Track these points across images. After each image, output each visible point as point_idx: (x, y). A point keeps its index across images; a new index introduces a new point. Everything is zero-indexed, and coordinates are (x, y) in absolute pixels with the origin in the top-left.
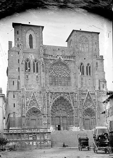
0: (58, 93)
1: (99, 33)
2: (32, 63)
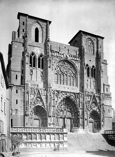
0: (64, 92)
2: (37, 57)
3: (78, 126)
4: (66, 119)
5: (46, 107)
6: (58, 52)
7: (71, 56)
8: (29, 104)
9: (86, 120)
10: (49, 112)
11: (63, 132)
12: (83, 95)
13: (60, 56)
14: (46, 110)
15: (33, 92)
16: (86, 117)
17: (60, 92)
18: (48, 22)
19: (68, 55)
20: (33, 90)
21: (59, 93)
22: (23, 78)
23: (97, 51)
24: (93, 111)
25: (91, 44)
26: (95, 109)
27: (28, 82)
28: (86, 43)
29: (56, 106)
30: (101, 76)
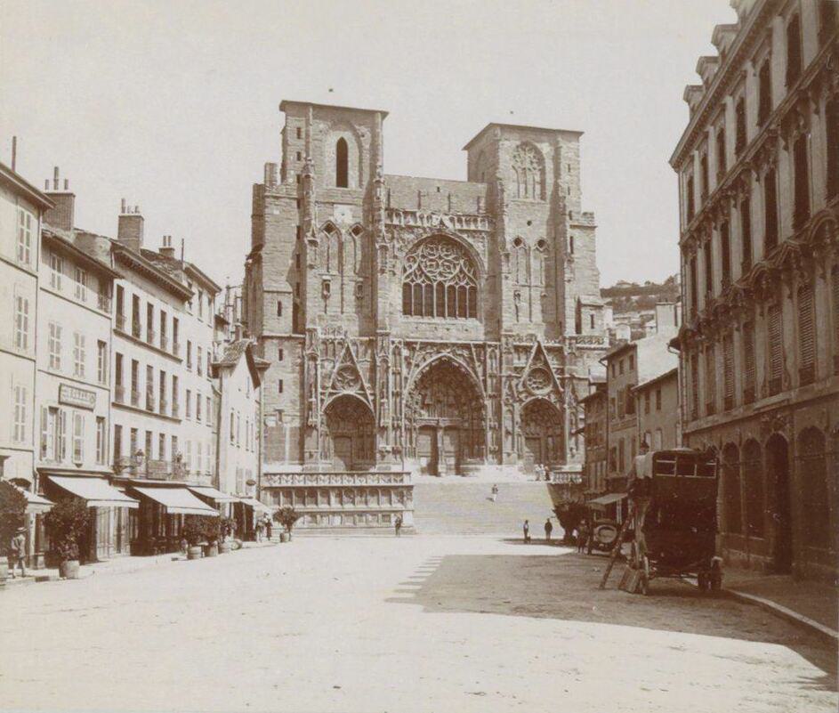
1: (581, 133)
3: (480, 455)
4: (440, 433)
5: (371, 398)
6: (413, 214)
7: (456, 218)
8: (316, 390)
9: (508, 433)
10: (380, 414)
11: (401, 484)
12: (497, 351)
13: (419, 224)
14: (372, 407)
15: (330, 353)
16: (507, 423)
17: (418, 347)
18: (371, 117)
19: (447, 217)
20: (330, 347)
21: (414, 349)
22: (298, 310)
23: (556, 186)
24: (537, 400)
25: (532, 163)
26: (543, 393)
27: (315, 324)
28: (512, 163)
29: (405, 392)
30: (567, 276)
